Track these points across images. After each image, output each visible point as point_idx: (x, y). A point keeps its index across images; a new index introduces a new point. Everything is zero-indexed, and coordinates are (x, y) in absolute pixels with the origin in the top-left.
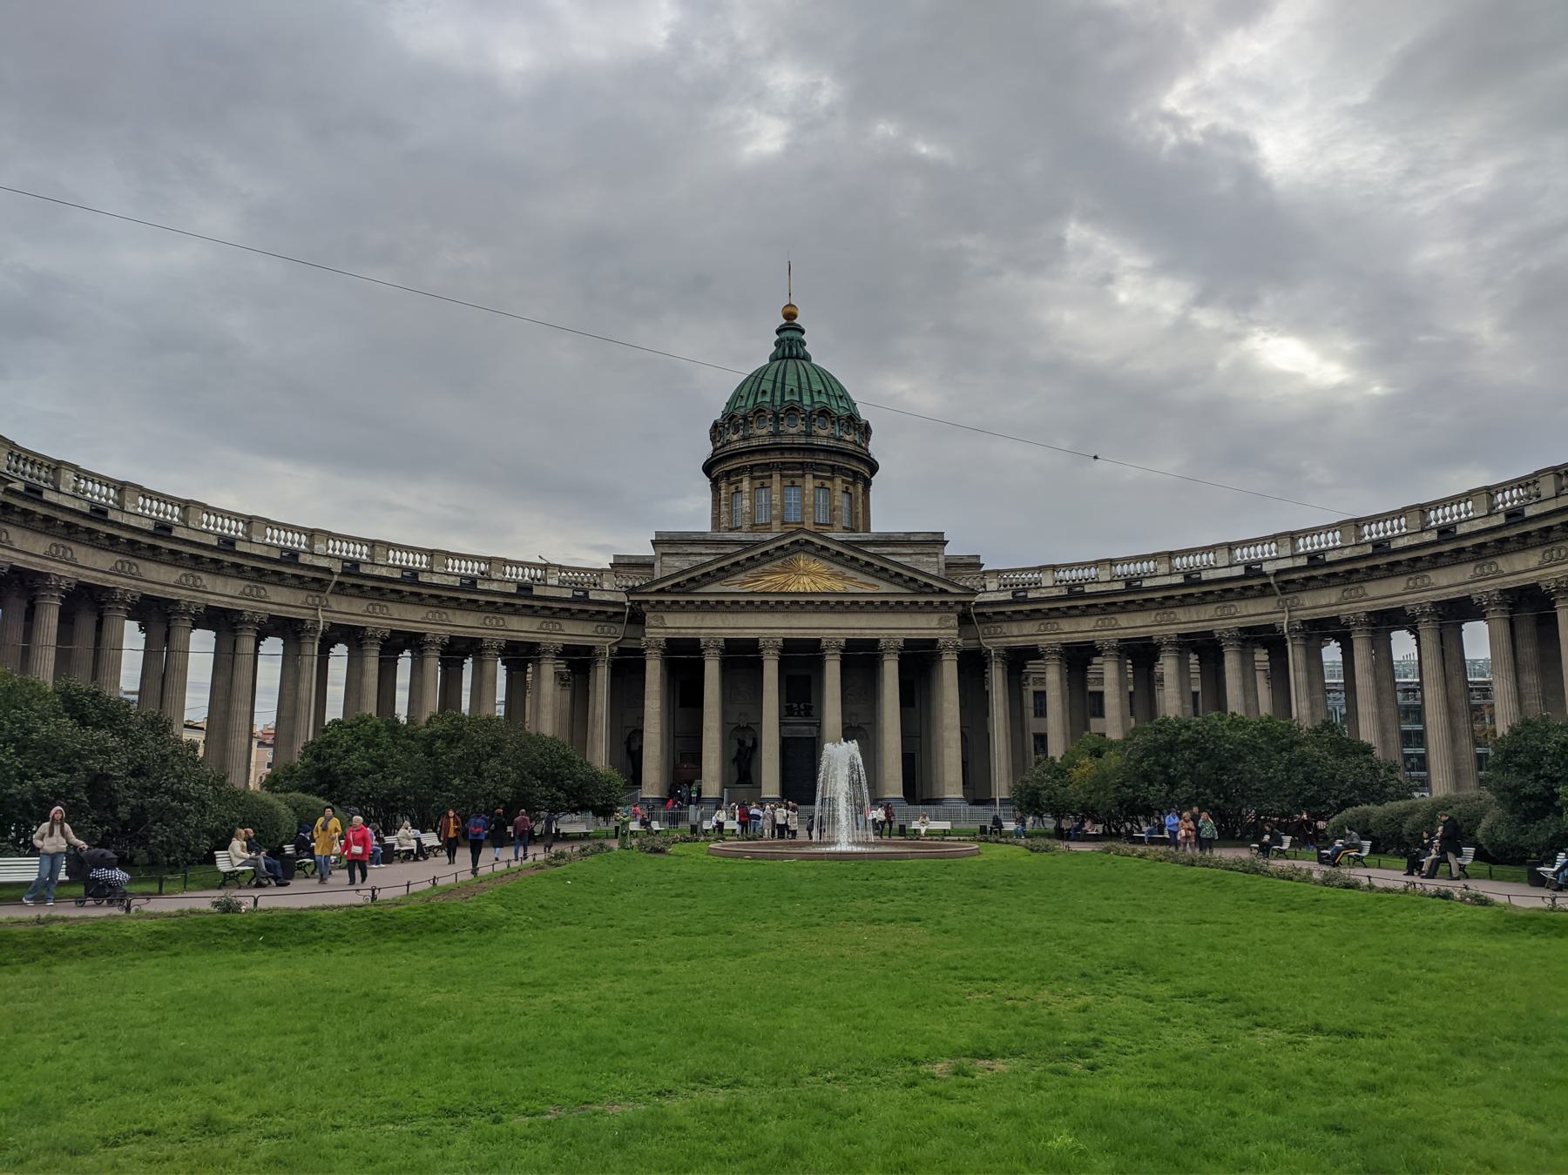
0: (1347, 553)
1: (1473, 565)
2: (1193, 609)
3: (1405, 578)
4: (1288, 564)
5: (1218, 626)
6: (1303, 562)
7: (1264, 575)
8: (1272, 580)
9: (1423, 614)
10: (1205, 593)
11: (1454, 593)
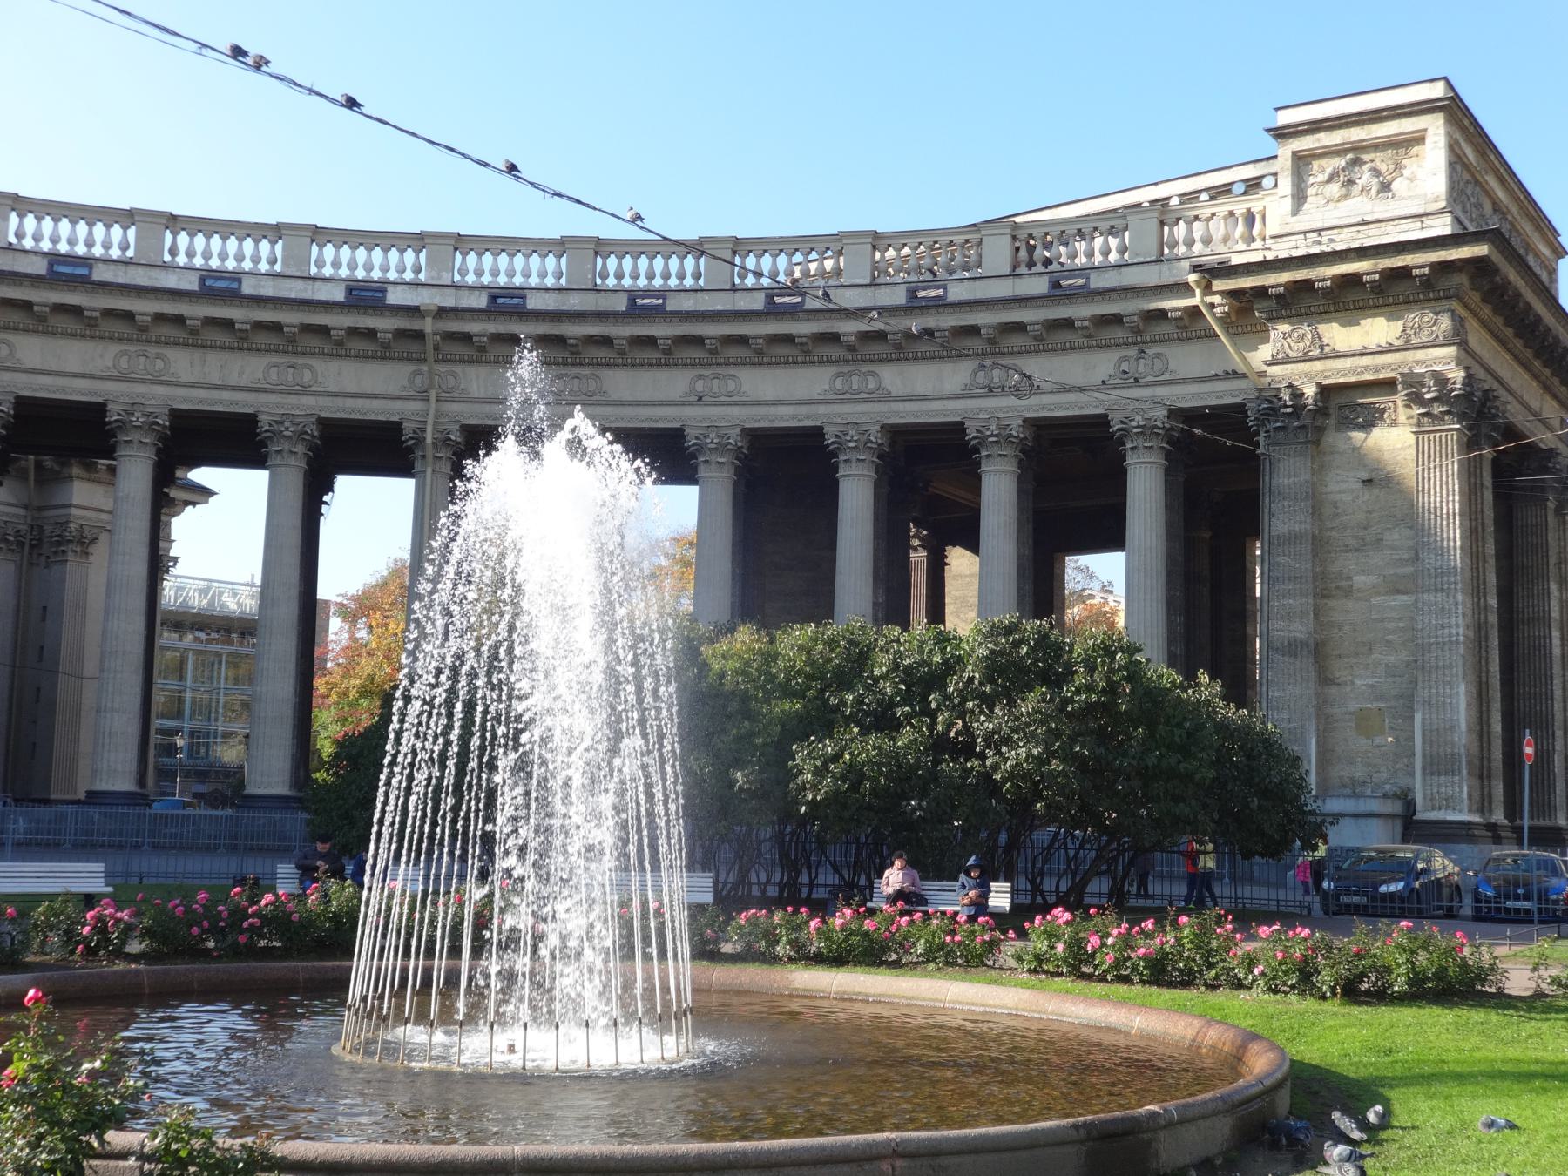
0: (574, 303)
1: (828, 372)
2: (214, 358)
3: (691, 373)
4: (449, 300)
5: (269, 408)
6: (481, 301)
7: (414, 311)
8: (428, 326)
9: (721, 448)
10: (259, 326)
11: (785, 417)
